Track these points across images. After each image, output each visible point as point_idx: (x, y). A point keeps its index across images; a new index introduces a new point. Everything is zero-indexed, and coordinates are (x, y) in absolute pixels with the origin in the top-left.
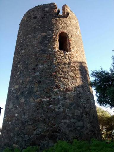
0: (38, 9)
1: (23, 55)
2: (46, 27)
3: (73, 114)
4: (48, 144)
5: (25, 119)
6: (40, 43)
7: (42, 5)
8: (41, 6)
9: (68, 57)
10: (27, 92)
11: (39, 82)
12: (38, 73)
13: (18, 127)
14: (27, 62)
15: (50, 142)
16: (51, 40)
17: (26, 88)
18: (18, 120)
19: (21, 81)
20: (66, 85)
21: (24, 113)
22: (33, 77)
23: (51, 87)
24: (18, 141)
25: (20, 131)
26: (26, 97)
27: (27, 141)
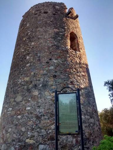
0: (48, 5)
1: (33, 47)
2: (58, 24)
3: (87, 111)
4: (67, 139)
5: (41, 113)
6: (53, 38)
7: (52, 2)
8: (52, 3)
9: (79, 56)
10: (41, 85)
11: (55, 76)
12: (52, 68)
13: (32, 122)
14: (39, 55)
15: (69, 137)
16: (64, 37)
17: (39, 80)
18: (31, 113)
19: (32, 73)
20: (79, 83)
21: (39, 107)
22: (47, 71)
23: (66, 83)
24: (33, 136)
25: (35, 125)
26: (40, 90)
27: (44, 135)
